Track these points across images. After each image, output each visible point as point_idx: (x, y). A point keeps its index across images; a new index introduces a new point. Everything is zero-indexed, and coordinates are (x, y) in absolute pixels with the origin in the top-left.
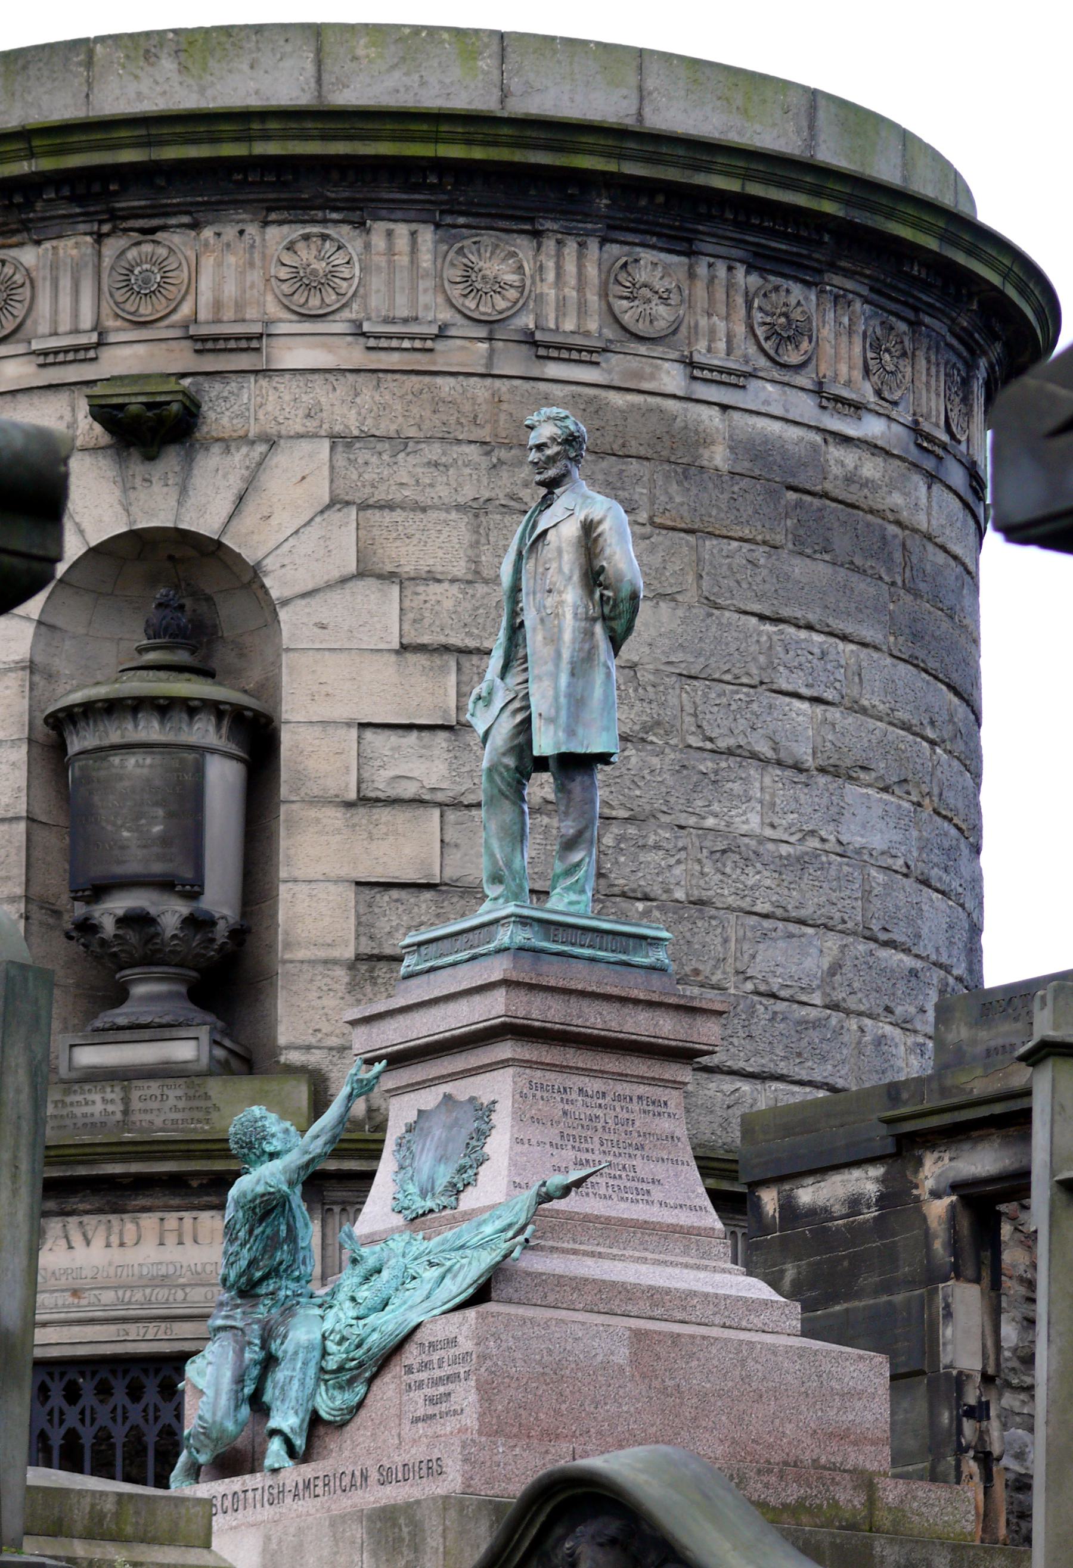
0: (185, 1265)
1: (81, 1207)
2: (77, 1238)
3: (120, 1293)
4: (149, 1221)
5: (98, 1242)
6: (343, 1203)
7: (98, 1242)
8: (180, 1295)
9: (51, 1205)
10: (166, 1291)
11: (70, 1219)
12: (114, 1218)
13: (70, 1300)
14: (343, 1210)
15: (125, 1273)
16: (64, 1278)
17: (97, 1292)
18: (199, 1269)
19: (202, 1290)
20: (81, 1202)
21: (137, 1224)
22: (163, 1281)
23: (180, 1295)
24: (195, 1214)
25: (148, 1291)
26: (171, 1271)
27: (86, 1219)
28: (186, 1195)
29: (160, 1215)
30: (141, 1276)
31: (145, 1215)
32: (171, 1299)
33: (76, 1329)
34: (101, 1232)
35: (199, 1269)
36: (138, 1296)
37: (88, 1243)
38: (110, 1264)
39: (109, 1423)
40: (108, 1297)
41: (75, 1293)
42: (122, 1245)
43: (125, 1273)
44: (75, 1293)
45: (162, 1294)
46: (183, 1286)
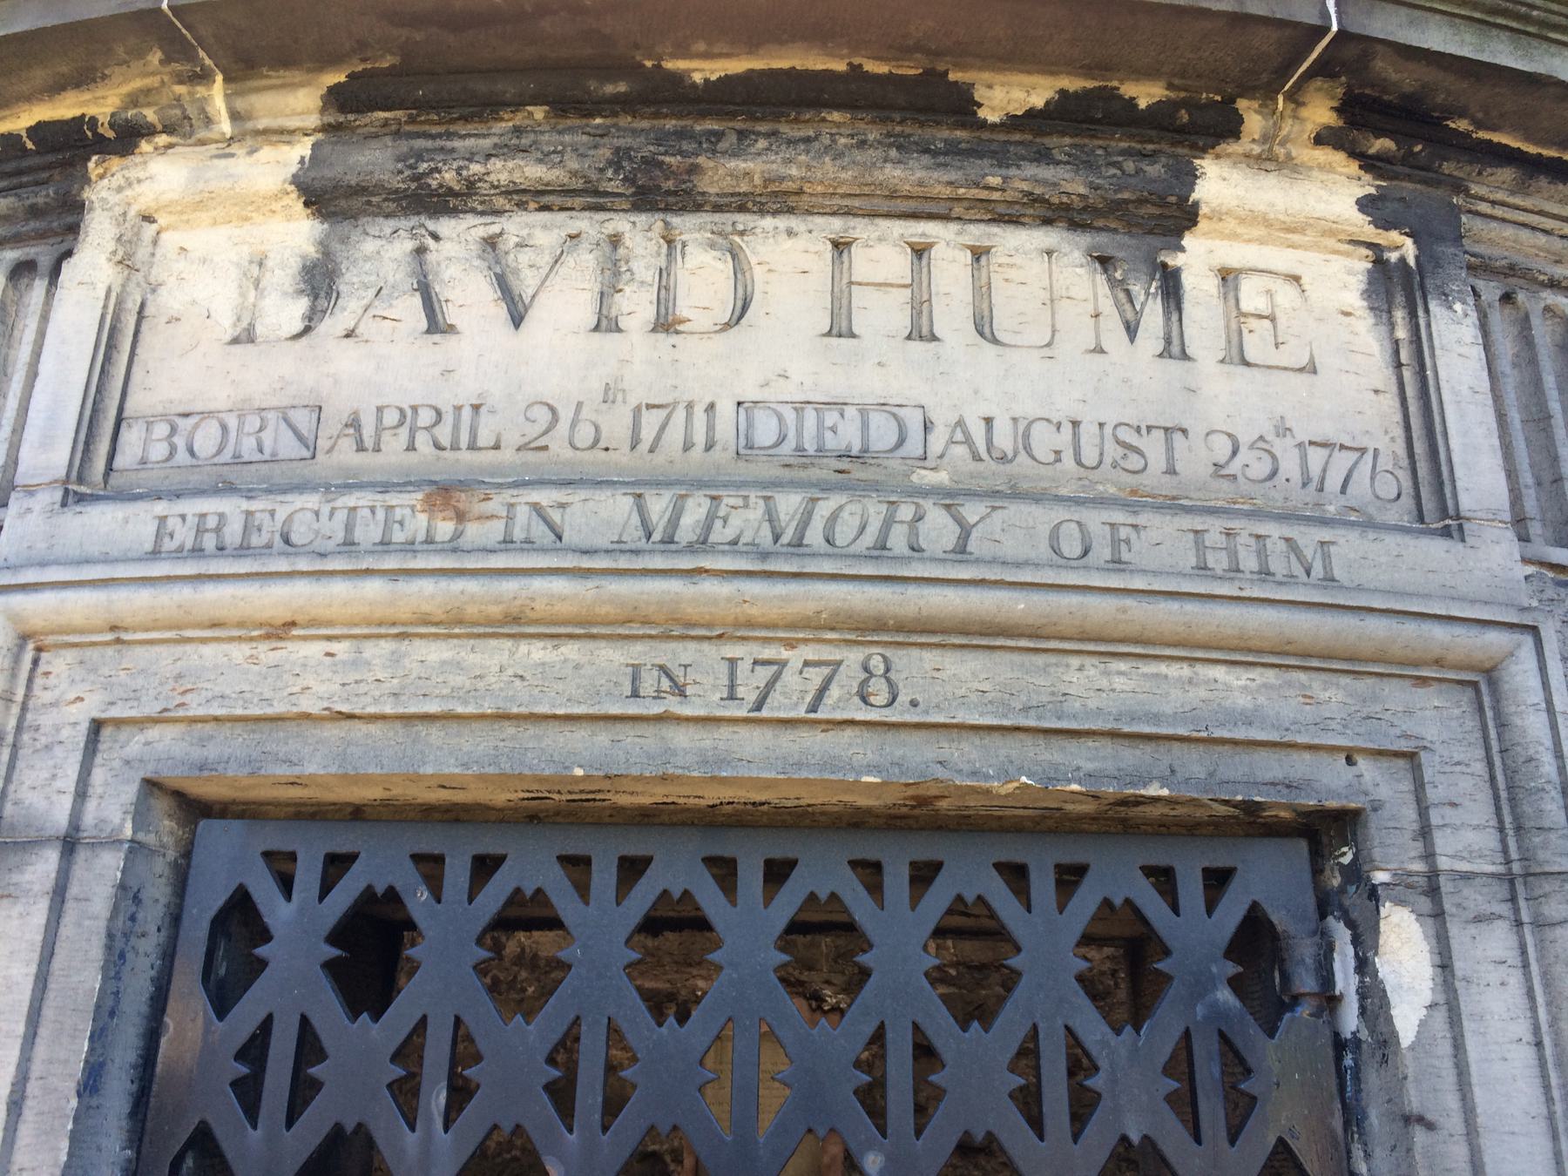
0: (943, 420)
1: (502, 171)
2: (468, 292)
3: (659, 505)
4: (787, 254)
5: (565, 302)
6: (1512, 270)
7: (565, 302)
8: (938, 528)
9: (375, 160)
10: (875, 511)
11: (445, 226)
12: (639, 234)
13: (419, 523)
14: (1507, 298)
15: (675, 434)
16: (394, 444)
17: (544, 497)
18: (1004, 439)
19: (1043, 518)
20: (502, 150)
21: (735, 254)
22: (851, 470)
23: (938, 528)
24: (977, 233)
25: (789, 504)
26: (883, 434)
27: (514, 226)
28: (954, 149)
29: (837, 224)
30: (747, 449)
31: (768, 222)
32: (898, 541)
33: (435, 653)
34: (583, 268)
35: (1004, 439)
36: (745, 520)
37: (517, 320)
38: (609, 396)
39: (539, 1113)
40: (601, 515)
41: (444, 493)
42: (666, 324)
43: (675, 434)
44: (444, 493)
45: (855, 518)
46: (949, 498)
